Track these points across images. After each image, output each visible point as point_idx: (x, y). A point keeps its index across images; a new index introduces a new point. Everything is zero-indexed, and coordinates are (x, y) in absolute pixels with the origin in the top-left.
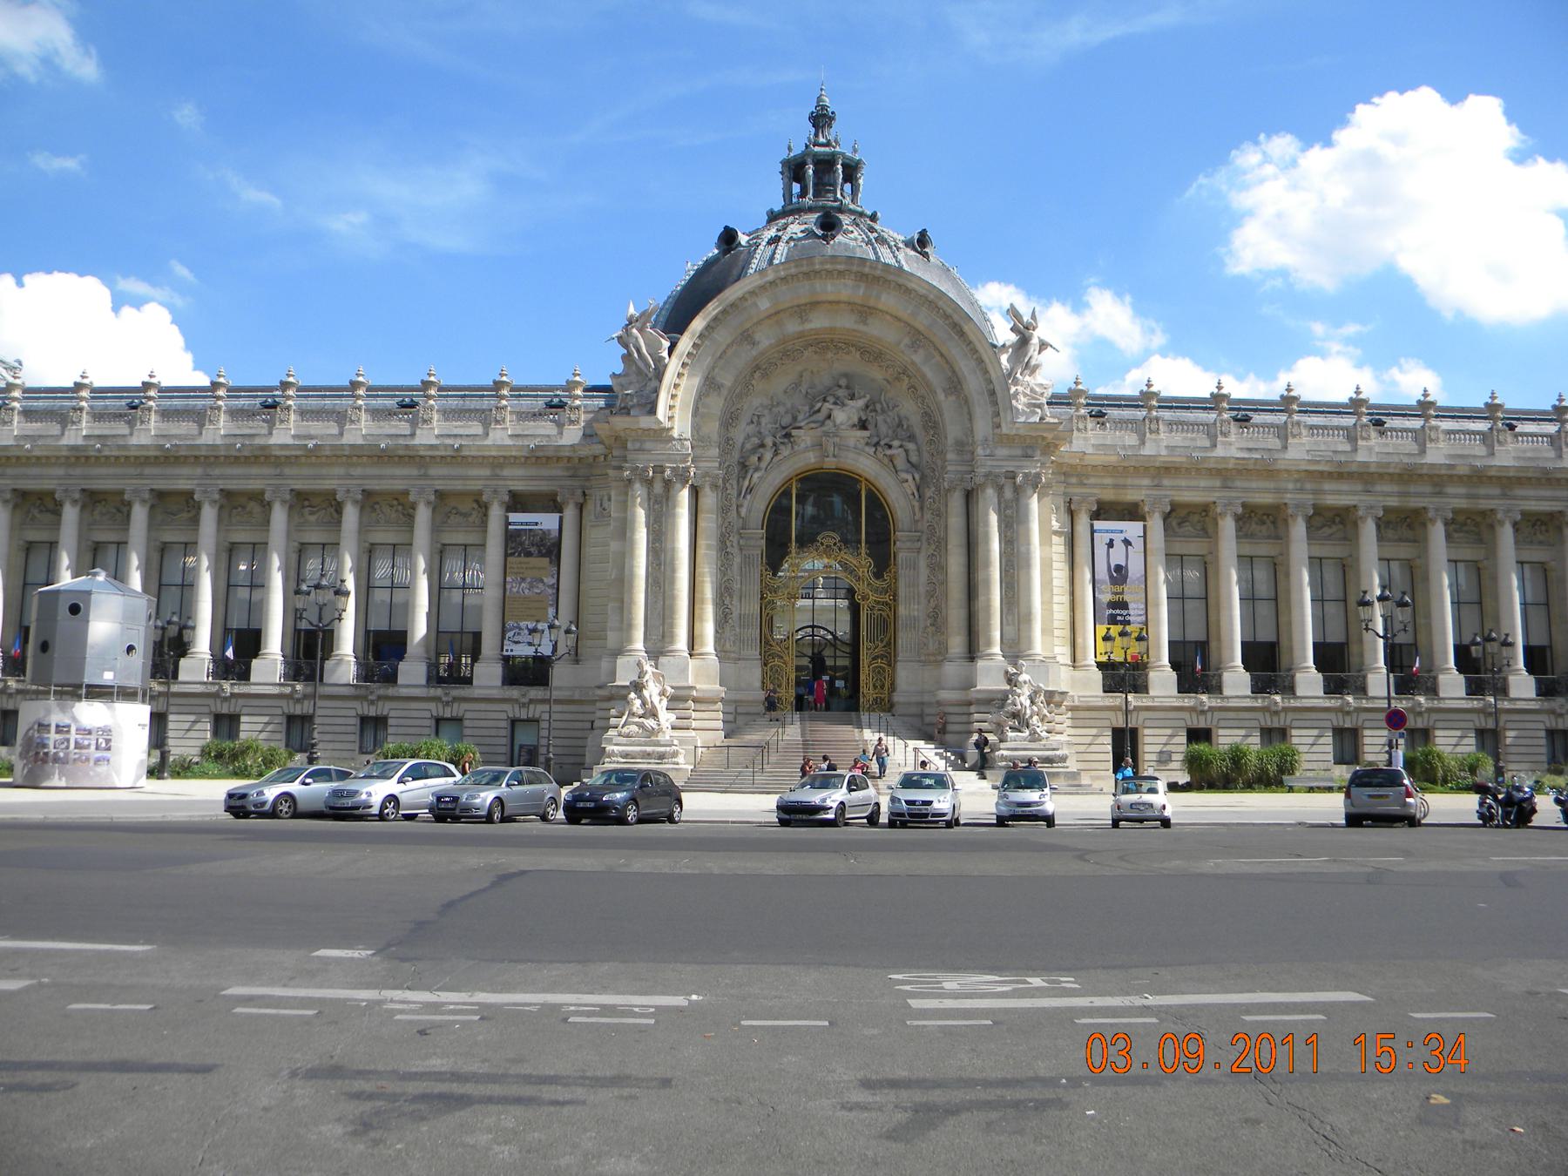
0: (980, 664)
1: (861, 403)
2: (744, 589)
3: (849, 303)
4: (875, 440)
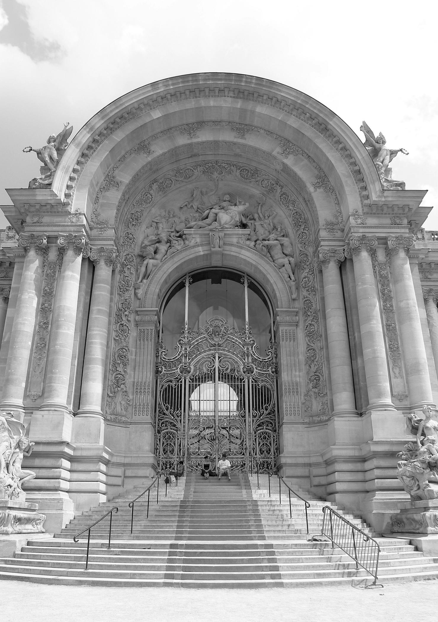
0: (375, 415)
1: (241, 208)
2: (138, 358)
3: (229, 122)
4: (254, 238)
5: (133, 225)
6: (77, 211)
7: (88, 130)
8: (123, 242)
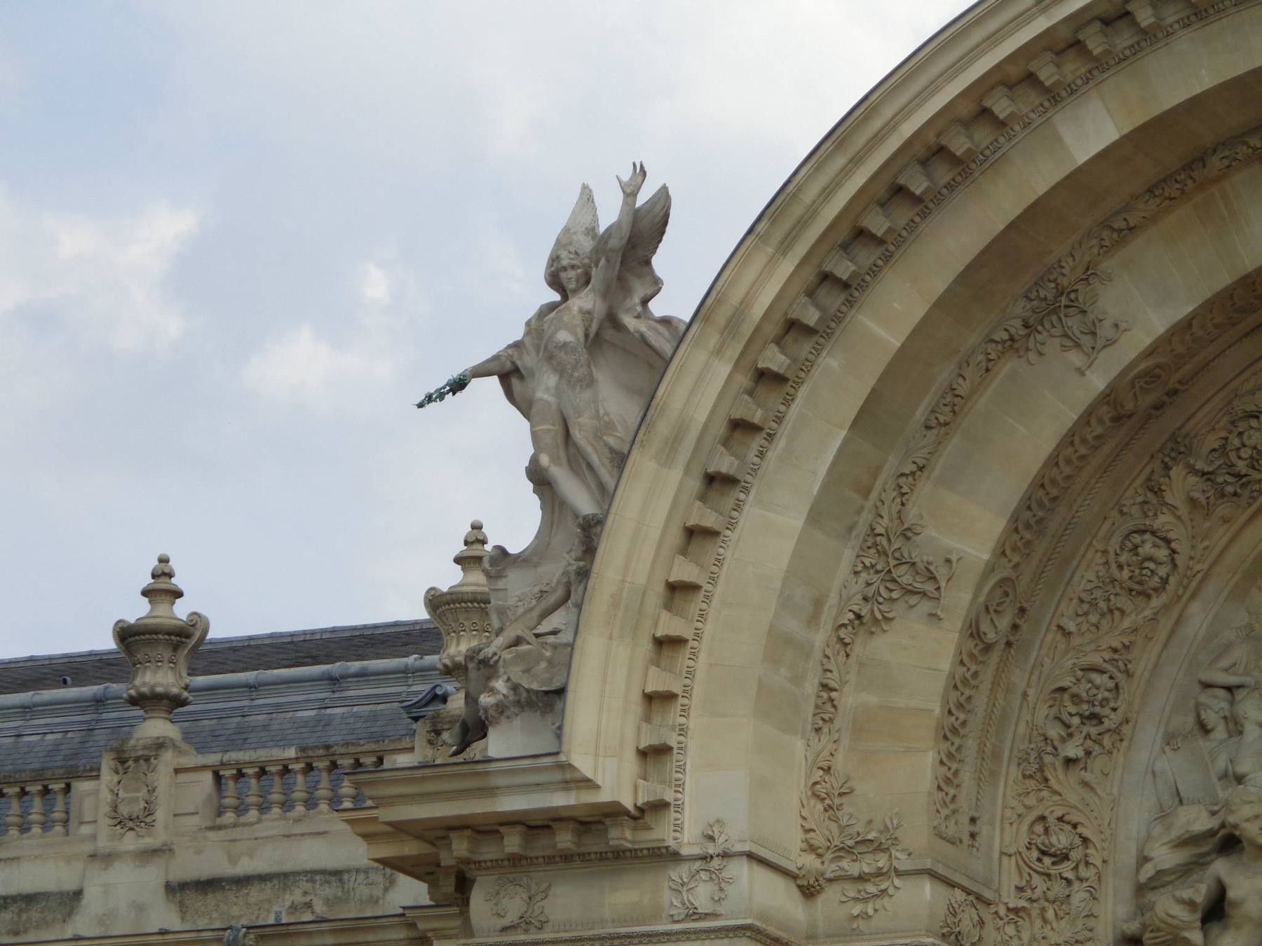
5: (1069, 762)
6: (711, 838)
7: (713, 340)
8: (1020, 889)
